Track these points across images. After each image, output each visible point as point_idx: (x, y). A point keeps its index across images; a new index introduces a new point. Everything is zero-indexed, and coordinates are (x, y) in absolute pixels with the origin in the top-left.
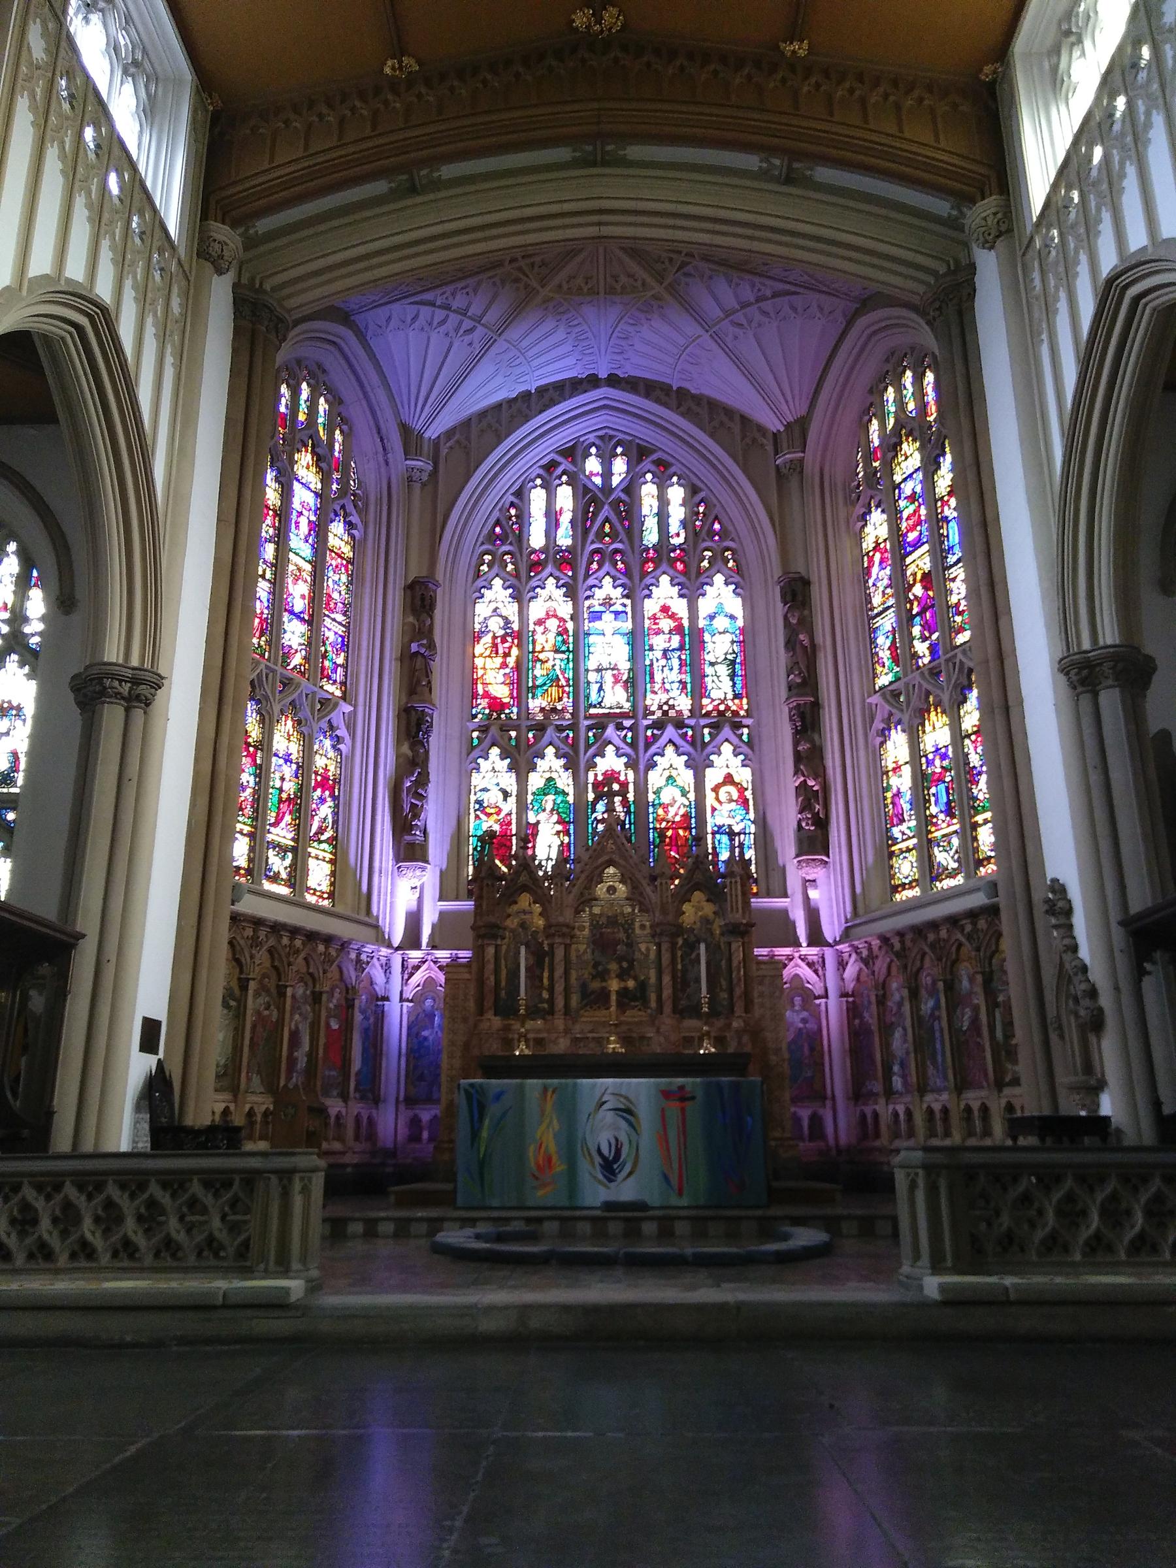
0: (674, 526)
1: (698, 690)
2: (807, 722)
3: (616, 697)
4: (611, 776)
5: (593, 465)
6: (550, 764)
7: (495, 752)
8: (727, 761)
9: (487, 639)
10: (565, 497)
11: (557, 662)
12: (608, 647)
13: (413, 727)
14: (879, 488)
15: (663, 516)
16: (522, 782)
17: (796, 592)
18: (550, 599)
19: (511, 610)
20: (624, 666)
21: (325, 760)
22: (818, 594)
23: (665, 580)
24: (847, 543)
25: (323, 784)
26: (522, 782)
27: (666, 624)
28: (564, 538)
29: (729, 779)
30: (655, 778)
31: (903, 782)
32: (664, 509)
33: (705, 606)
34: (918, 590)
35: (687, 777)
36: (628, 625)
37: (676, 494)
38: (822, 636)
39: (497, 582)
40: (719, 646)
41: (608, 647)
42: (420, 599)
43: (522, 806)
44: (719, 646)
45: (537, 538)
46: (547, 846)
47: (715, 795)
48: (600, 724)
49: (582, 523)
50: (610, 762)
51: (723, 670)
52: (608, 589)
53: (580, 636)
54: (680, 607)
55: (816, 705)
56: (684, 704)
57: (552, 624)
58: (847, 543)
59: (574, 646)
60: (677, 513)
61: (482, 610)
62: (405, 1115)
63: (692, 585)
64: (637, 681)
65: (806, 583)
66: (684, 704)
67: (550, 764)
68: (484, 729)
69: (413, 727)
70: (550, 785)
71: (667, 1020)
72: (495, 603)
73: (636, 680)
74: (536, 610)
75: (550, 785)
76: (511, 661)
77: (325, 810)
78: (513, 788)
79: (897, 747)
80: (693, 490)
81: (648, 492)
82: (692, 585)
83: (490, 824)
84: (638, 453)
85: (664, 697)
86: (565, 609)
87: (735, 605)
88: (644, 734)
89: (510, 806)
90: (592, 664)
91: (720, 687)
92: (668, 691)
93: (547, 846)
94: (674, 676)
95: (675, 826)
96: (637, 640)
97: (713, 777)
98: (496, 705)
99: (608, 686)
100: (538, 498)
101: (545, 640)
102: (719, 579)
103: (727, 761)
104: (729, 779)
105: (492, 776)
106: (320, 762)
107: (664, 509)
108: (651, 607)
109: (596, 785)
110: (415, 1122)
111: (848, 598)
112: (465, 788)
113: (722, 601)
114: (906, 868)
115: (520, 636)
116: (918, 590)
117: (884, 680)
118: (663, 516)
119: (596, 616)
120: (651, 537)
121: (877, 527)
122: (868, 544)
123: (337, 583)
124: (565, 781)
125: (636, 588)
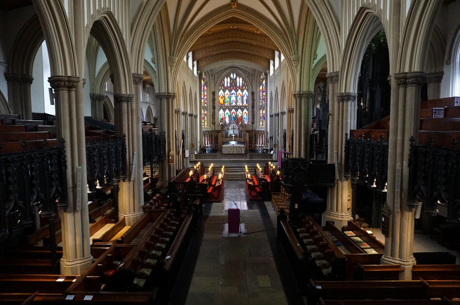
0: (241, 84)
1: (243, 103)
2: (253, 107)
3: (234, 104)
4: (233, 112)
5: (232, 76)
6: (227, 111)
7: (222, 109)
8: (245, 110)
9: (220, 97)
10: (229, 79)
11: (228, 99)
12: (233, 98)
13: (214, 108)
14: (261, 84)
15: (239, 82)
16: (224, 112)
17: (253, 94)
18: (227, 92)
19: (223, 93)
20: (235, 100)
21: (206, 112)
22: (255, 94)
23: (239, 90)
24: (258, 88)
25: (206, 115)
26: (224, 112)
27: (239, 95)
28: (229, 85)
29: (245, 113)
30: (238, 112)
31: (261, 115)
32: (240, 81)
33: (244, 93)
34: (264, 97)
35: (241, 112)
36: (235, 95)
37: (241, 79)
38: (255, 98)
39: (221, 90)
40: (245, 98)
41: (233, 98)
42: (214, 94)
43: (224, 115)
44: (245, 98)
45: (226, 85)
46: (227, 121)
47: (244, 114)
48: (232, 106)
49: (231, 84)
50: (233, 110)
51: (245, 101)
52: (233, 91)
53: (230, 96)
54: (241, 93)
55: (254, 106)
56: (241, 104)
57: (227, 95)
58: (258, 88)
59: (230, 98)
60: (241, 82)
61: (220, 93)
62: (214, 145)
63: (242, 91)
64: (236, 102)
65: (254, 92)
66: (241, 104)
67: (227, 111)
68: (220, 107)
69: (214, 108)
70: (227, 113)
71: (238, 138)
72: (221, 92)
73: (236, 102)
74: (226, 93)
75: (227, 113)
76: (223, 99)
77: (206, 118)
78: (224, 113)
79: (261, 112)
80: (243, 80)
81: (238, 79)
82: (242, 91)
83: (221, 117)
84: (237, 75)
85: (239, 104)
86: (229, 93)
87: (247, 93)
88: (237, 108)
89: (223, 115)
90: (232, 100)
91: (245, 103)
92: (240, 104)
93: (227, 121)
94: (240, 101)
95: (240, 117)
96: (236, 97)
97: (244, 112)
98: (221, 104)
99: (233, 102)
100: (226, 79)
101: (227, 97)
102: (245, 90)
103: (245, 110)
104: (245, 113)
105: (221, 112)
106: (205, 113)
107: (240, 81)
108: (238, 93)
109: (232, 113)
110: (215, 146)
111: (258, 94)
112: (218, 113)
113: (245, 92)
114: (261, 123)
115: (224, 97)
116: (264, 97)
117: (261, 104)
118: (239, 82)
119: (232, 94)
120: (238, 85)
121: (261, 88)
122: (260, 89)
123: (205, 93)
124: (229, 113)
125: (236, 91)
